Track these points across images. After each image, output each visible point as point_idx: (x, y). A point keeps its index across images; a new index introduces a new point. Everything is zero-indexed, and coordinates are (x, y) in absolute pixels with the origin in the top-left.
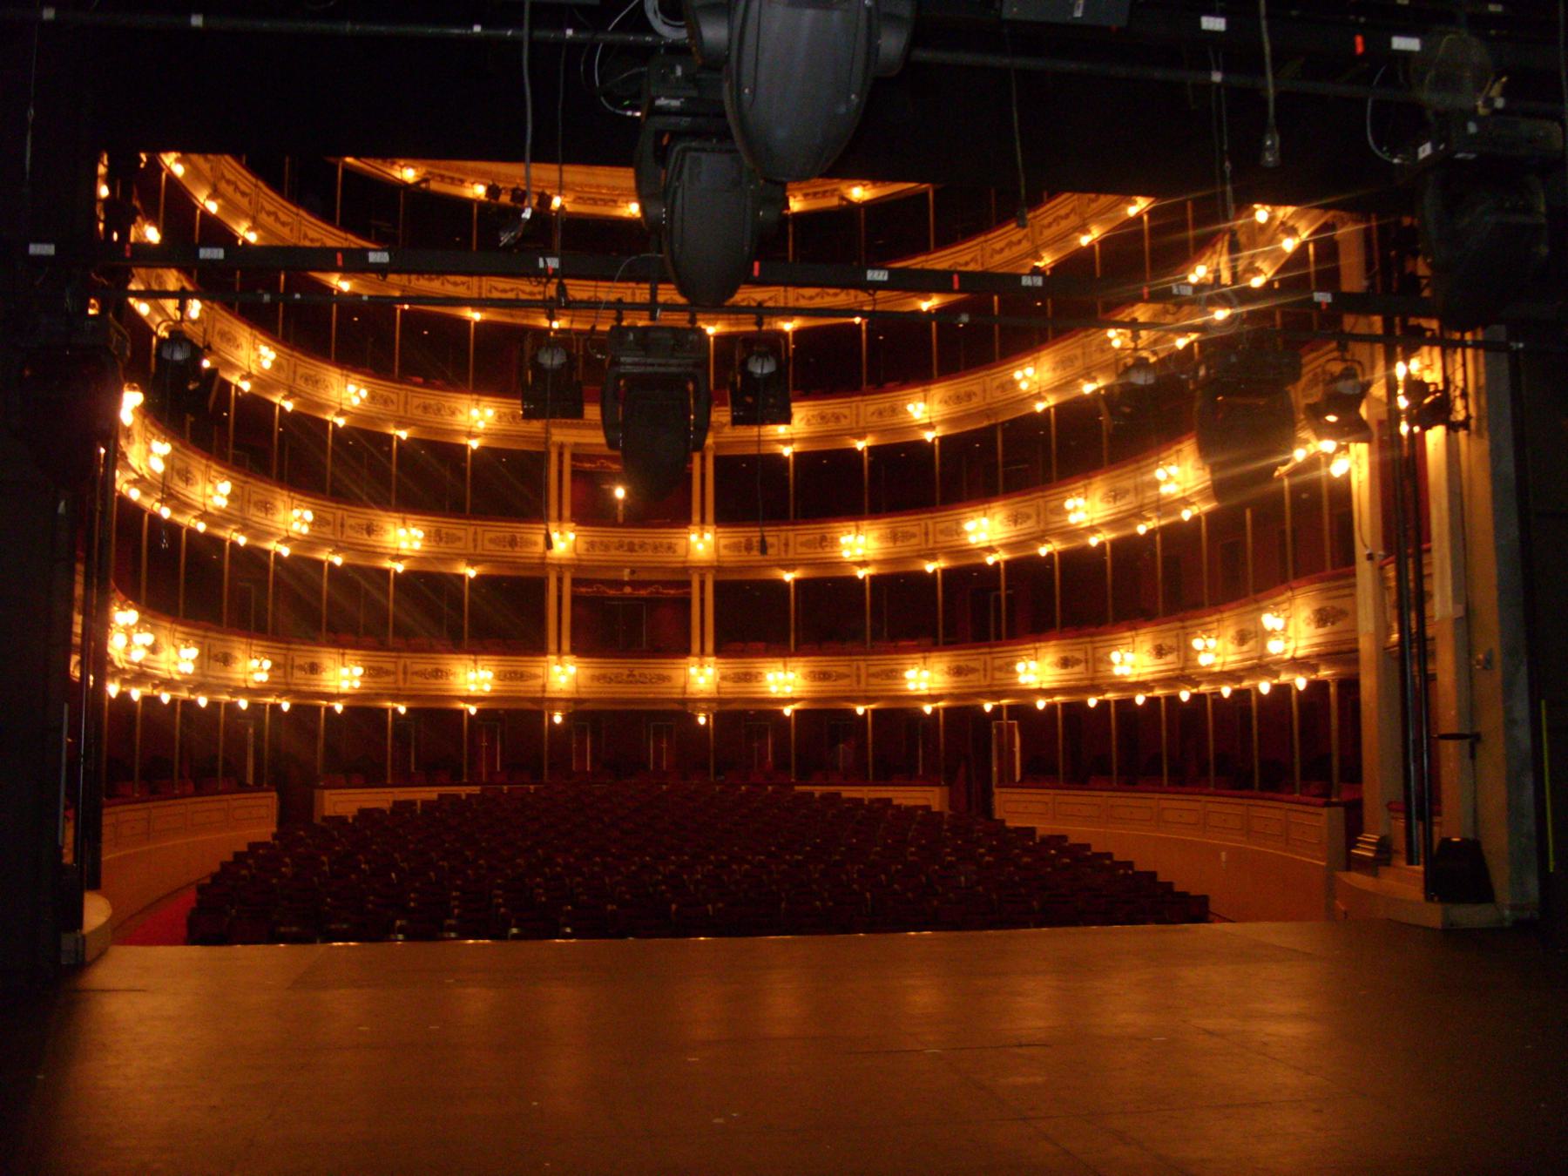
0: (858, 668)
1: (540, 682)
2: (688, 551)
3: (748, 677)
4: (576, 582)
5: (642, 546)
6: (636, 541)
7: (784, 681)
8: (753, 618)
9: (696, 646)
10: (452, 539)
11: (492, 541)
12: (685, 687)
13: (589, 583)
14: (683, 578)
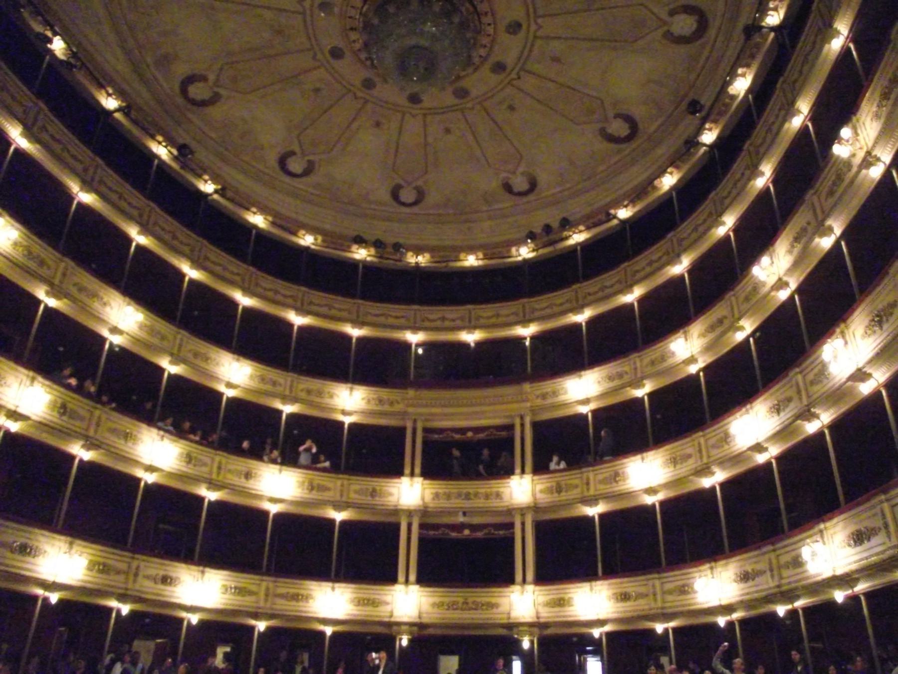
0: (653, 586)
1: (388, 608)
3: (561, 603)
4: (422, 526)
6: (471, 491)
7: (594, 603)
9: (519, 577)
10: (322, 488)
11: (356, 492)
12: (509, 613)
13: (436, 527)
14: (506, 520)
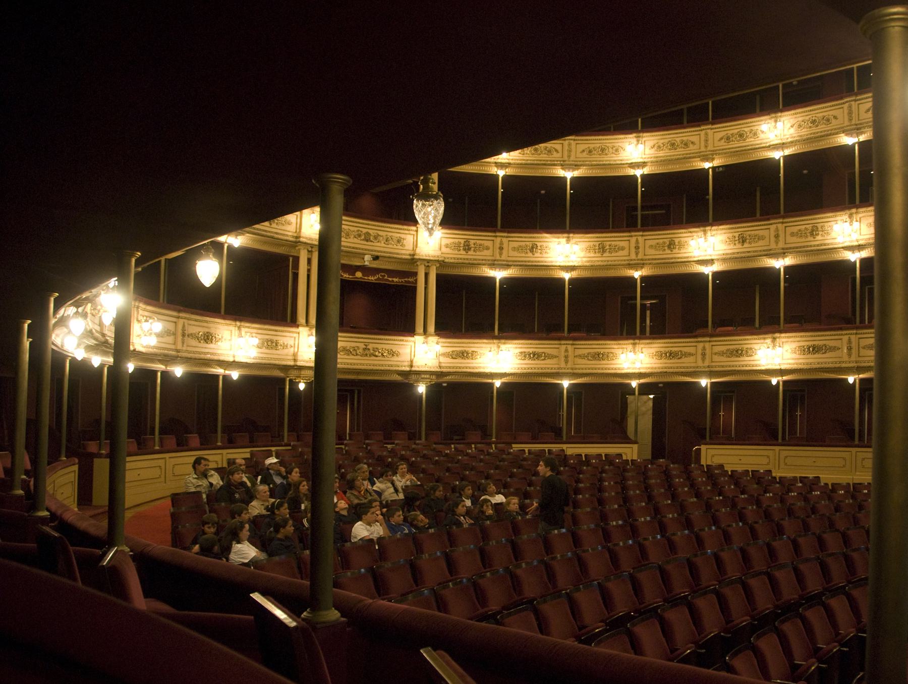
2: (416, 245)
5: (376, 237)
6: (371, 232)
8: (467, 307)
12: (412, 361)
